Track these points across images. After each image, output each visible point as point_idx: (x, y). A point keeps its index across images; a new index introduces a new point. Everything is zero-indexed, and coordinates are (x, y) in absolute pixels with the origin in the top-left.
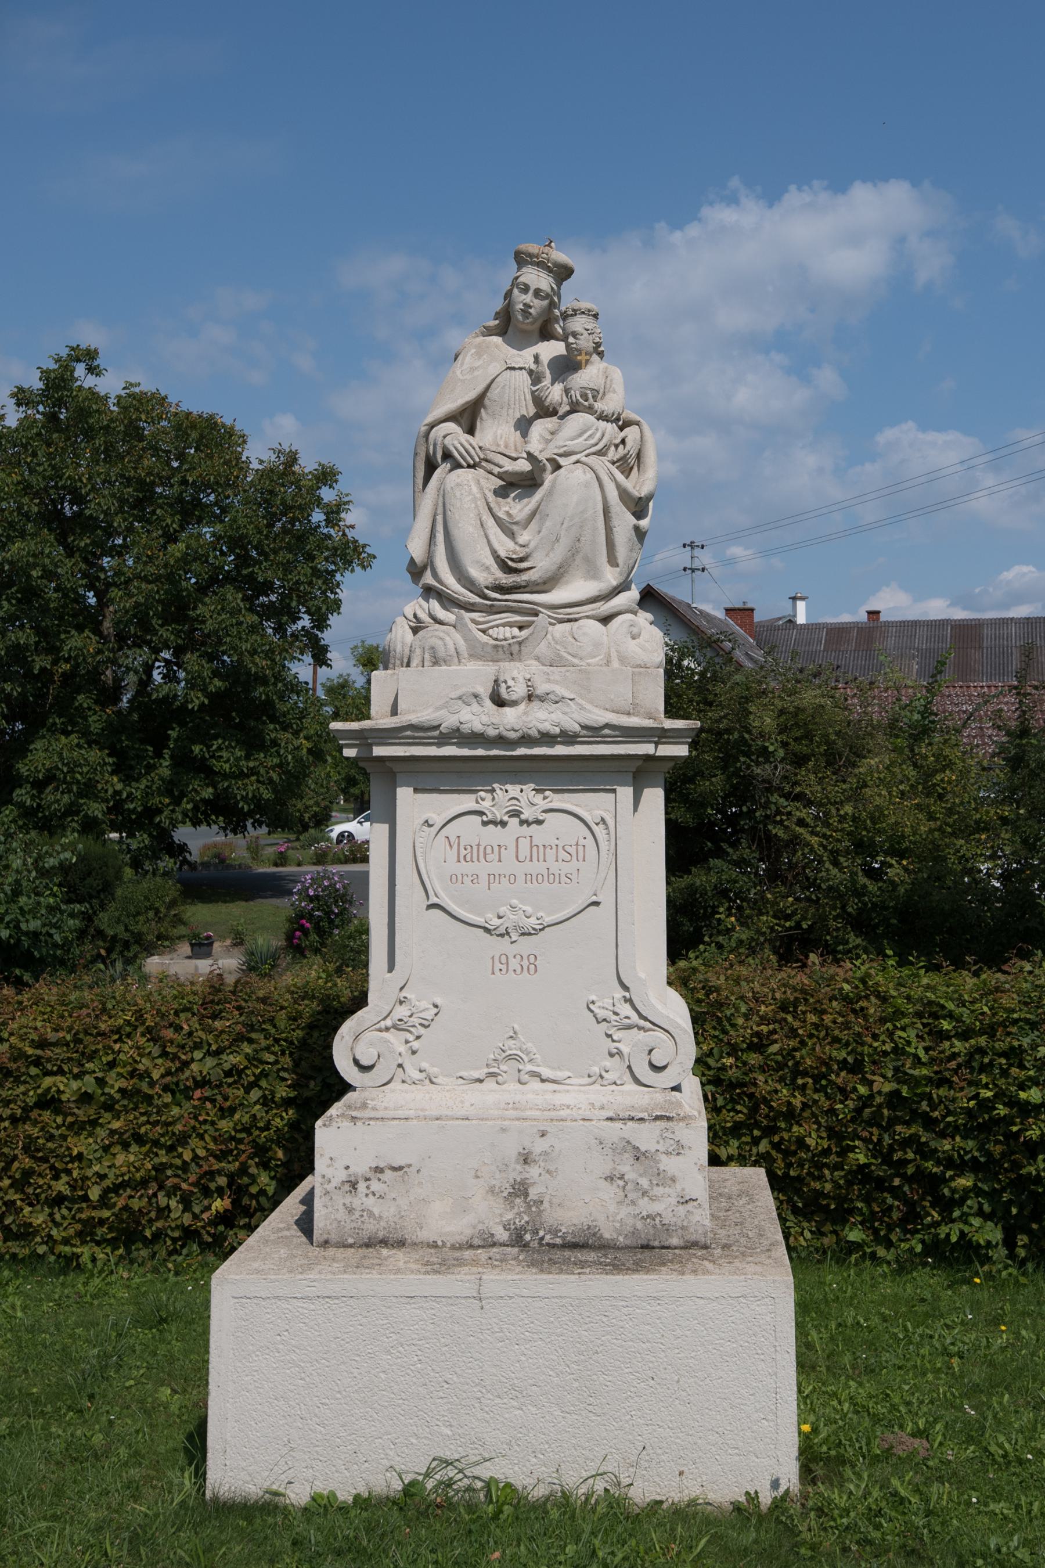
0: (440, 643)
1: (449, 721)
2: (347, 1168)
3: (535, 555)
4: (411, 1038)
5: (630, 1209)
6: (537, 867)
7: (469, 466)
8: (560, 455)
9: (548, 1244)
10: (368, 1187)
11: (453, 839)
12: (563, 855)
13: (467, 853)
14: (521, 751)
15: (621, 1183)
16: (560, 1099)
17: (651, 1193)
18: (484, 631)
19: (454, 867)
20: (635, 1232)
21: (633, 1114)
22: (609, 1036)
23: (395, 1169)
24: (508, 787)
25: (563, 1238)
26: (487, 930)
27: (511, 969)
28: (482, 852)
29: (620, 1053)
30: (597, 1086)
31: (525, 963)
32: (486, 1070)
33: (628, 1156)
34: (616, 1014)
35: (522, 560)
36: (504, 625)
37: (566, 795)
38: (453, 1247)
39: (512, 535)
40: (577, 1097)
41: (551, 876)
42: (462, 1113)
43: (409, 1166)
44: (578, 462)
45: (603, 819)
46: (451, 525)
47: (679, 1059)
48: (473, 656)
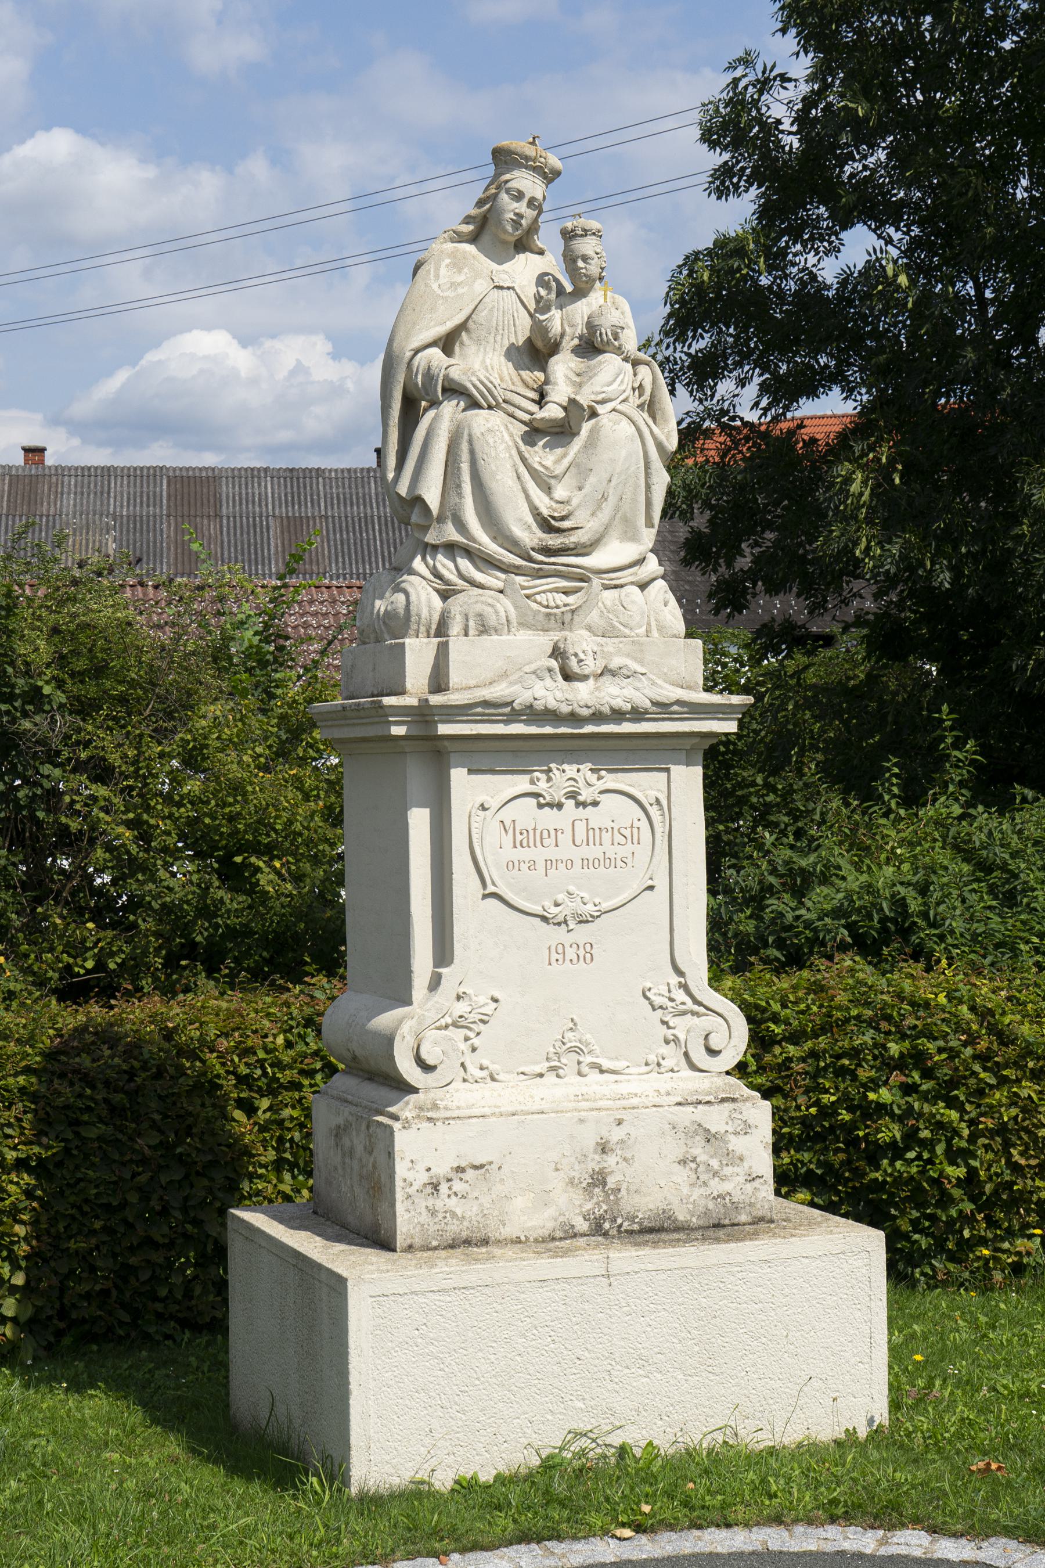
0: (490, 609)
1: (522, 697)
2: (428, 1170)
3: (576, 513)
4: (471, 1035)
5: (702, 1191)
6: (594, 852)
8: (597, 402)
9: (626, 1231)
10: (450, 1188)
11: (508, 823)
12: (618, 838)
13: (523, 838)
14: (589, 729)
15: (693, 1165)
16: (624, 1088)
17: (722, 1173)
18: (528, 597)
19: (510, 853)
20: (707, 1212)
21: (700, 1098)
22: (664, 1023)
23: (476, 1168)
24: (565, 766)
25: (641, 1224)
26: (544, 919)
27: (568, 958)
29: (676, 1040)
30: (654, 1075)
31: (581, 952)
32: (547, 1064)
33: (700, 1140)
34: (672, 1000)
35: (563, 518)
36: (551, 591)
37: (620, 775)
38: (536, 1241)
39: (548, 490)
40: (640, 1085)
41: (607, 861)
42: (536, 1107)
43: (491, 1163)
44: (614, 410)
45: (658, 801)
46: (486, 477)
47: (733, 1042)
48: (523, 625)
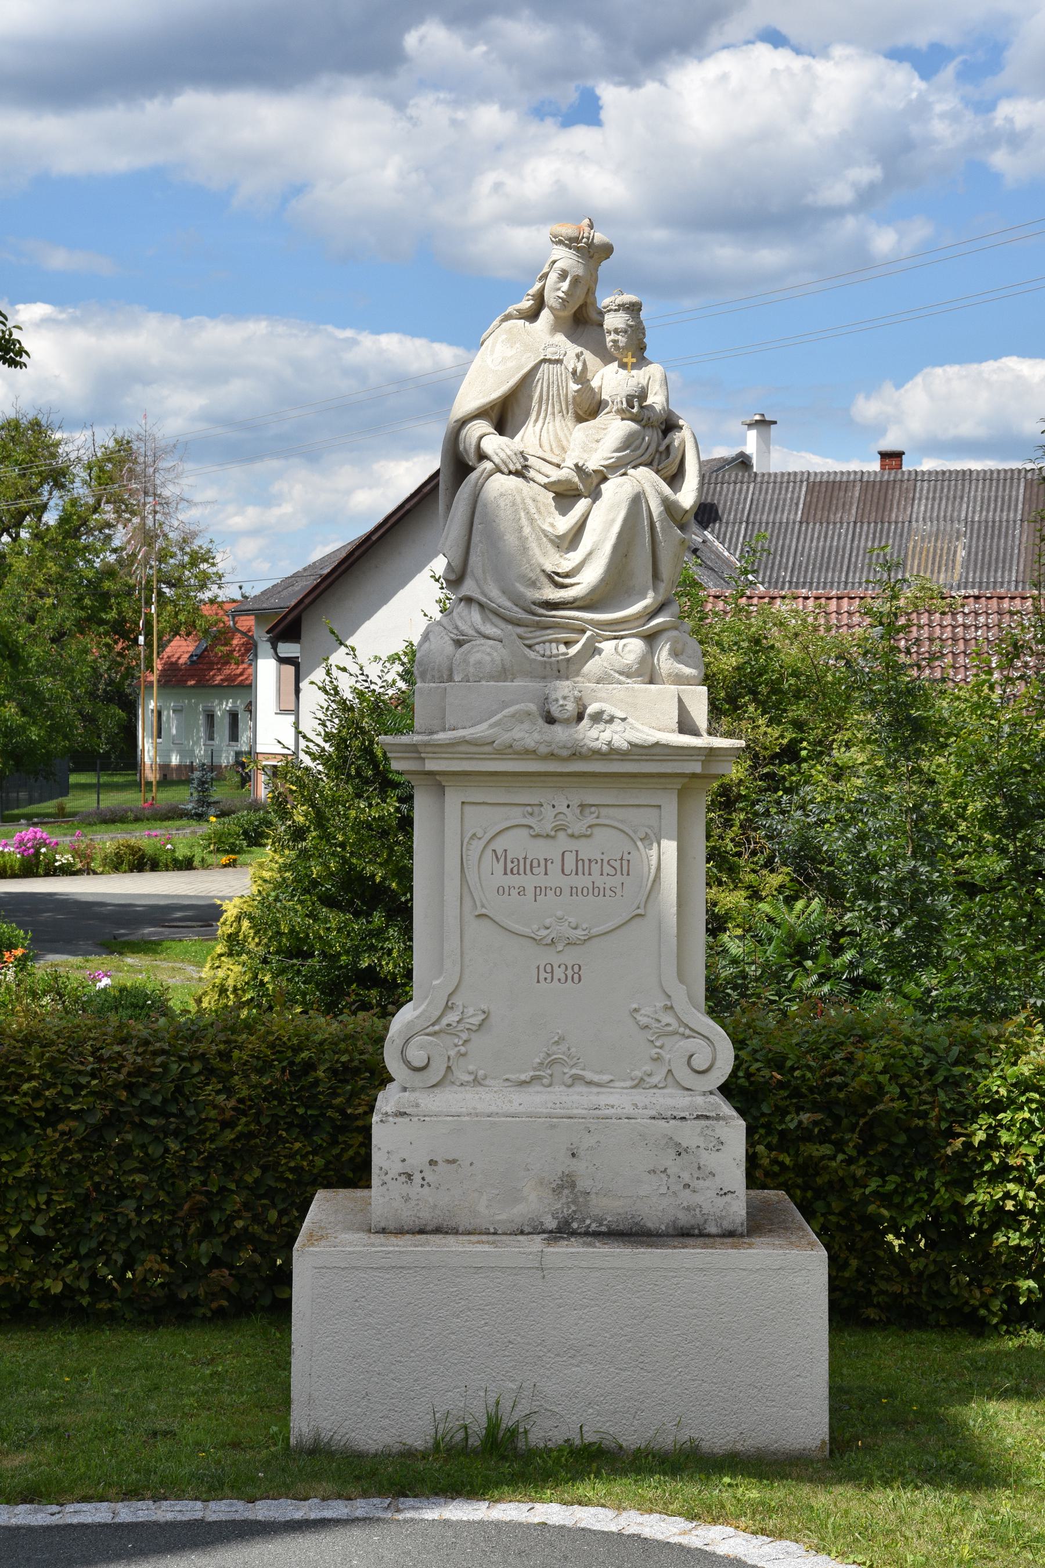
2: (404, 1160)
11: (500, 853)
12: (607, 869)
13: (514, 866)
18: (530, 647)
19: (500, 879)
28: (529, 866)
31: (570, 973)
33: (672, 1153)
35: (567, 575)
41: (595, 890)
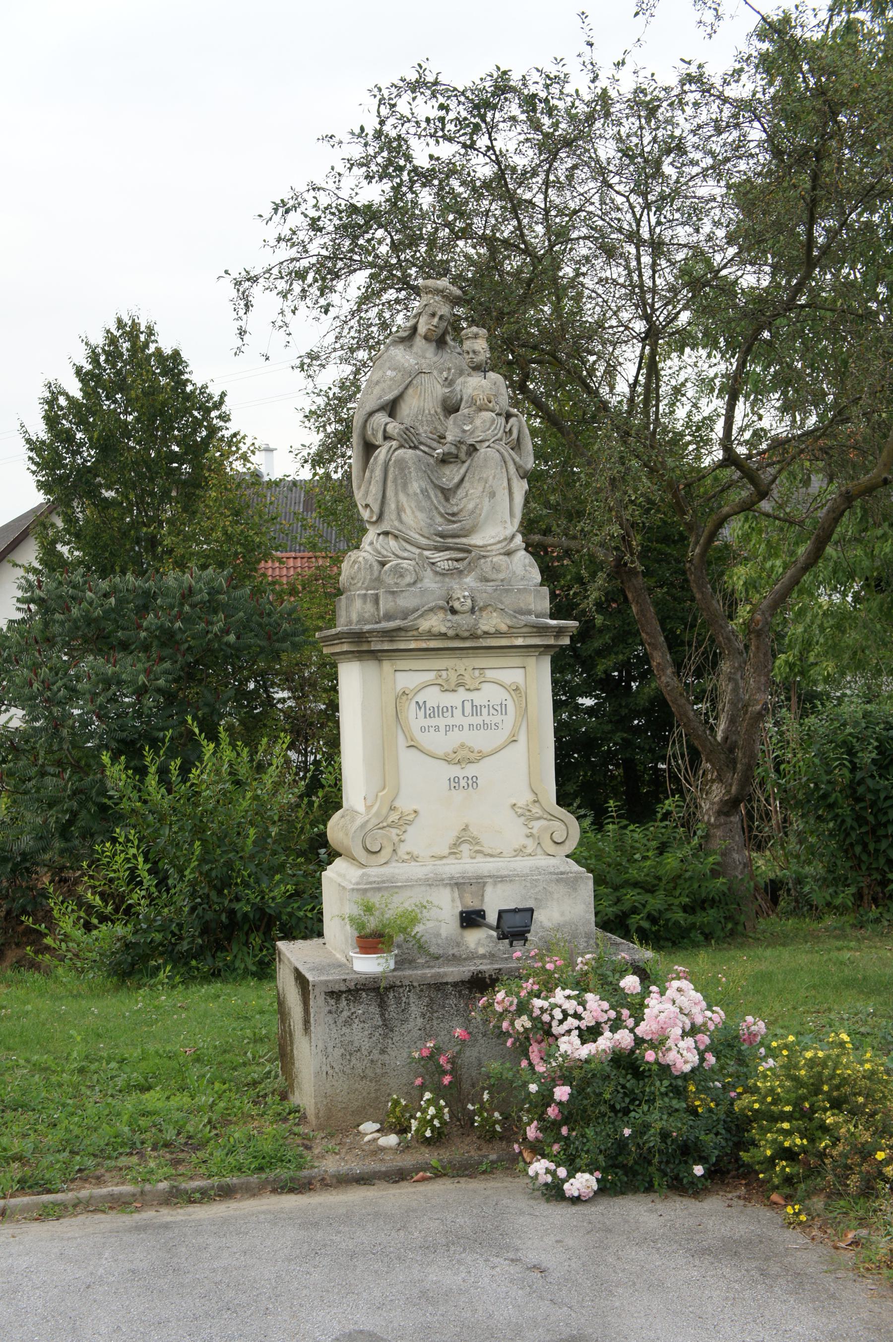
7: (410, 447)
12: (492, 711)
31: (470, 782)
41: (485, 726)
